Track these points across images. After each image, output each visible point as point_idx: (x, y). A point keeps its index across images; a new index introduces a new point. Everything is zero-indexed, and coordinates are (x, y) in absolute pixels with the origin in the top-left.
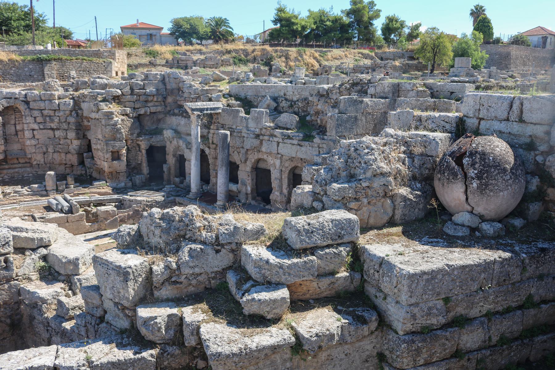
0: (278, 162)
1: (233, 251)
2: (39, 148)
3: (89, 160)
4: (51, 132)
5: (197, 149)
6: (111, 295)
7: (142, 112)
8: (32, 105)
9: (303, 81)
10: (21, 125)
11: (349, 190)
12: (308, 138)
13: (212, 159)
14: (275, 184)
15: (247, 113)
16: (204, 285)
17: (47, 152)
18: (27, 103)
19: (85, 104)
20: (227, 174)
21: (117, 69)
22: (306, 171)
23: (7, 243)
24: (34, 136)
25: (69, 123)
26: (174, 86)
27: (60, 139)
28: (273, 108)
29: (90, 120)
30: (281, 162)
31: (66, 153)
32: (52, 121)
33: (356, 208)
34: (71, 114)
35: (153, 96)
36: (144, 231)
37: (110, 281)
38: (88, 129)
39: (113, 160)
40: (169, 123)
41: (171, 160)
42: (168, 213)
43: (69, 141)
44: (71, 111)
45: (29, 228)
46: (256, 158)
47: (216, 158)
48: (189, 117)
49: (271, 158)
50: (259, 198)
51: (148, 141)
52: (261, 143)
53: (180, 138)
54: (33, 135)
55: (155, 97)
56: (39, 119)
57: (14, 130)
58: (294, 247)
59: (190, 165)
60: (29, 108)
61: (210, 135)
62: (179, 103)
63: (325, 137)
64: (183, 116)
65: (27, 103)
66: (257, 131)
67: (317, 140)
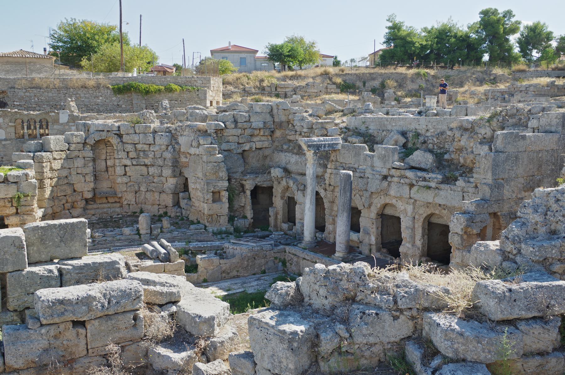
0: (410, 208)
1: (413, 318)
2: (130, 186)
3: (186, 201)
4: (144, 168)
5: (312, 191)
6: (270, 365)
7: (247, 148)
8: (125, 138)
9: (435, 112)
10: (112, 161)
11: (552, 250)
12: (449, 180)
13: (328, 203)
14: (405, 234)
15: (372, 150)
16: (378, 358)
17: (139, 190)
18: (120, 136)
19: (184, 137)
20: (348, 221)
21: (211, 99)
22: (455, 220)
23: (138, 298)
24: (125, 175)
25: (165, 159)
26: (284, 118)
27: (153, 177)
28: (402, 144)
29: (188, 156)
30: (414, 208)
31: (160, 193)
32: (146, 156)
33: (560, 272)
34: (167, 149)
35: (260, 129)
36: (305, 290)
37: (269, 348)
38: (187, 166)
39: (214, 201)
40: (277, 160)
41: (278, 203)
42: (334, 270)
43: (164, 179)
44: (168, 146)
45: (157, 280)
46: (383, 202)
47: (333, 202)
48: (305, 154)
49: (401, 204)
50: (384, 250)
51: (254, 180)
52: (389, 185)
53: (291, 178)
54: (125, 171)
55: (262, 130)
56: (132, 155)
57: (105, 166)
58: (493, 317)
59: (303, 211)
60: (122, 141)
61: (327, 176)
62: (289, 137)
63: (472, 180)
64: (293, 153)
65: (120, 136)
66: (385, 172)
67: (460, 183)
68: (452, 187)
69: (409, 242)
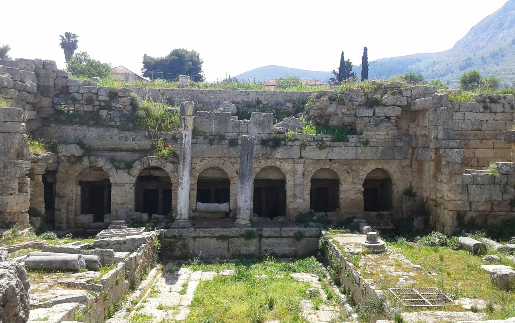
49: (287, 164)
63: (361, 136)
68: (346, 143)
69: (300, 198)
